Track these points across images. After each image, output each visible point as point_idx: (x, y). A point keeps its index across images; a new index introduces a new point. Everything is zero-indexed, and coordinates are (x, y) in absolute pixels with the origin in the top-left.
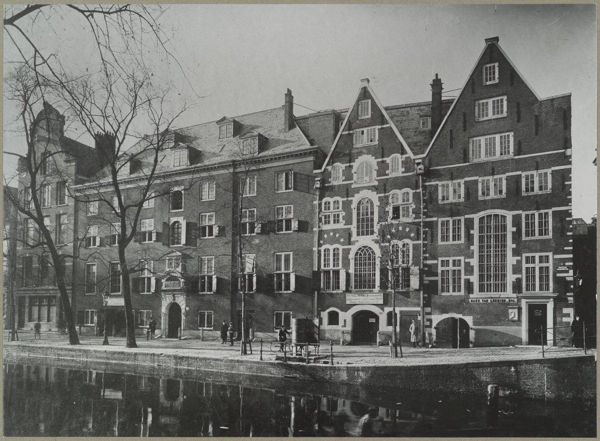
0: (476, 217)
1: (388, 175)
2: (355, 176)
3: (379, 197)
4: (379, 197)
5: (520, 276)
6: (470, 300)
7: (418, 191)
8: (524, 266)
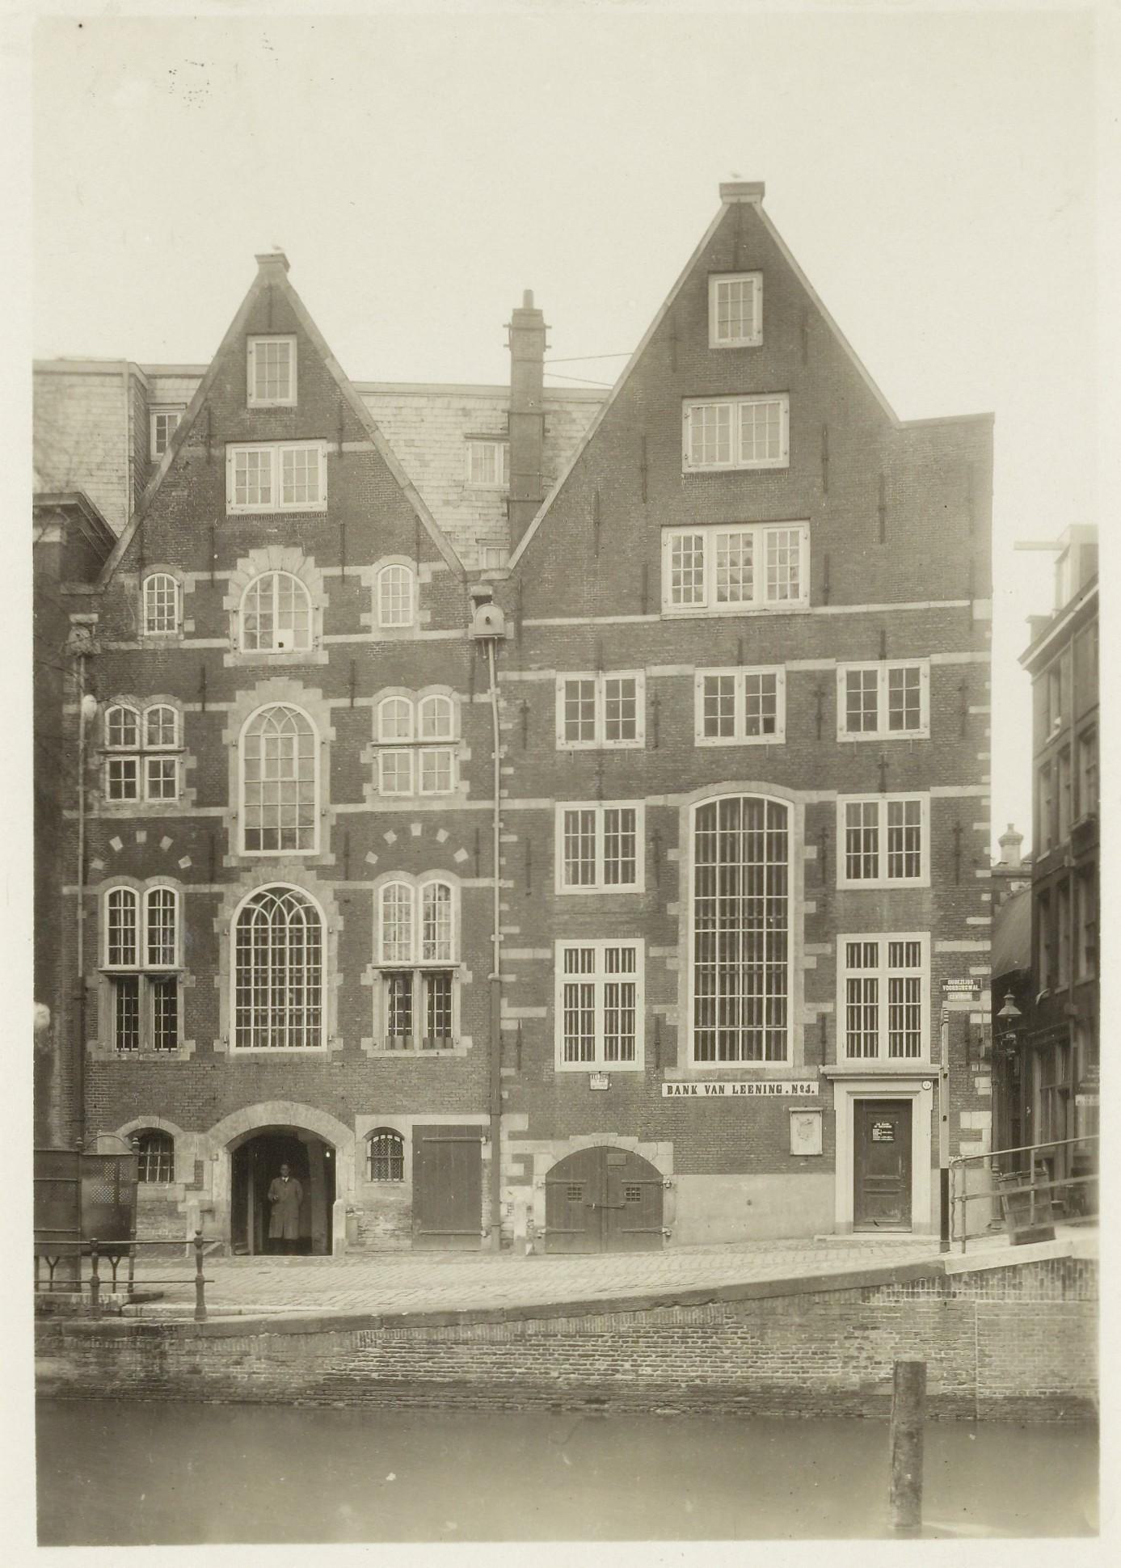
0: (689, 806)
1: (367, 629)
2: (238, 627)
3: (334, 711)
4: (334, 711)
5: (827, 1008)
6: (665, 1087)
7: (481, 698)
8: (844, 973)
